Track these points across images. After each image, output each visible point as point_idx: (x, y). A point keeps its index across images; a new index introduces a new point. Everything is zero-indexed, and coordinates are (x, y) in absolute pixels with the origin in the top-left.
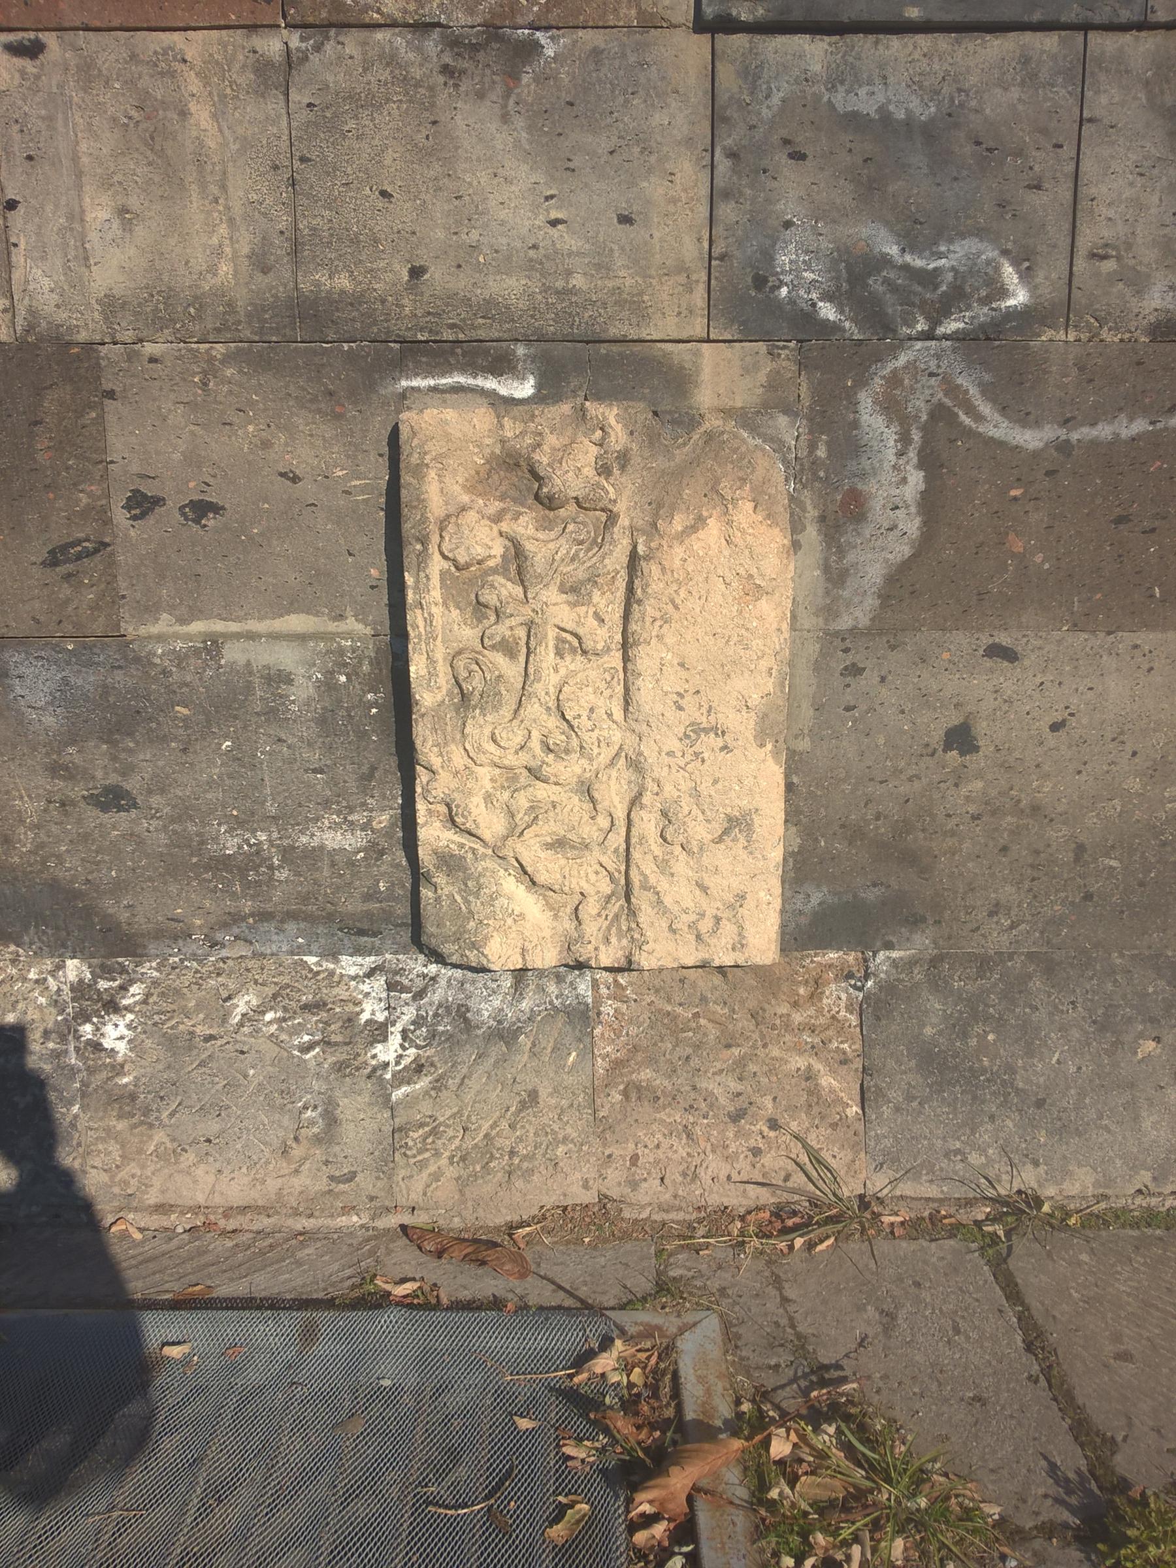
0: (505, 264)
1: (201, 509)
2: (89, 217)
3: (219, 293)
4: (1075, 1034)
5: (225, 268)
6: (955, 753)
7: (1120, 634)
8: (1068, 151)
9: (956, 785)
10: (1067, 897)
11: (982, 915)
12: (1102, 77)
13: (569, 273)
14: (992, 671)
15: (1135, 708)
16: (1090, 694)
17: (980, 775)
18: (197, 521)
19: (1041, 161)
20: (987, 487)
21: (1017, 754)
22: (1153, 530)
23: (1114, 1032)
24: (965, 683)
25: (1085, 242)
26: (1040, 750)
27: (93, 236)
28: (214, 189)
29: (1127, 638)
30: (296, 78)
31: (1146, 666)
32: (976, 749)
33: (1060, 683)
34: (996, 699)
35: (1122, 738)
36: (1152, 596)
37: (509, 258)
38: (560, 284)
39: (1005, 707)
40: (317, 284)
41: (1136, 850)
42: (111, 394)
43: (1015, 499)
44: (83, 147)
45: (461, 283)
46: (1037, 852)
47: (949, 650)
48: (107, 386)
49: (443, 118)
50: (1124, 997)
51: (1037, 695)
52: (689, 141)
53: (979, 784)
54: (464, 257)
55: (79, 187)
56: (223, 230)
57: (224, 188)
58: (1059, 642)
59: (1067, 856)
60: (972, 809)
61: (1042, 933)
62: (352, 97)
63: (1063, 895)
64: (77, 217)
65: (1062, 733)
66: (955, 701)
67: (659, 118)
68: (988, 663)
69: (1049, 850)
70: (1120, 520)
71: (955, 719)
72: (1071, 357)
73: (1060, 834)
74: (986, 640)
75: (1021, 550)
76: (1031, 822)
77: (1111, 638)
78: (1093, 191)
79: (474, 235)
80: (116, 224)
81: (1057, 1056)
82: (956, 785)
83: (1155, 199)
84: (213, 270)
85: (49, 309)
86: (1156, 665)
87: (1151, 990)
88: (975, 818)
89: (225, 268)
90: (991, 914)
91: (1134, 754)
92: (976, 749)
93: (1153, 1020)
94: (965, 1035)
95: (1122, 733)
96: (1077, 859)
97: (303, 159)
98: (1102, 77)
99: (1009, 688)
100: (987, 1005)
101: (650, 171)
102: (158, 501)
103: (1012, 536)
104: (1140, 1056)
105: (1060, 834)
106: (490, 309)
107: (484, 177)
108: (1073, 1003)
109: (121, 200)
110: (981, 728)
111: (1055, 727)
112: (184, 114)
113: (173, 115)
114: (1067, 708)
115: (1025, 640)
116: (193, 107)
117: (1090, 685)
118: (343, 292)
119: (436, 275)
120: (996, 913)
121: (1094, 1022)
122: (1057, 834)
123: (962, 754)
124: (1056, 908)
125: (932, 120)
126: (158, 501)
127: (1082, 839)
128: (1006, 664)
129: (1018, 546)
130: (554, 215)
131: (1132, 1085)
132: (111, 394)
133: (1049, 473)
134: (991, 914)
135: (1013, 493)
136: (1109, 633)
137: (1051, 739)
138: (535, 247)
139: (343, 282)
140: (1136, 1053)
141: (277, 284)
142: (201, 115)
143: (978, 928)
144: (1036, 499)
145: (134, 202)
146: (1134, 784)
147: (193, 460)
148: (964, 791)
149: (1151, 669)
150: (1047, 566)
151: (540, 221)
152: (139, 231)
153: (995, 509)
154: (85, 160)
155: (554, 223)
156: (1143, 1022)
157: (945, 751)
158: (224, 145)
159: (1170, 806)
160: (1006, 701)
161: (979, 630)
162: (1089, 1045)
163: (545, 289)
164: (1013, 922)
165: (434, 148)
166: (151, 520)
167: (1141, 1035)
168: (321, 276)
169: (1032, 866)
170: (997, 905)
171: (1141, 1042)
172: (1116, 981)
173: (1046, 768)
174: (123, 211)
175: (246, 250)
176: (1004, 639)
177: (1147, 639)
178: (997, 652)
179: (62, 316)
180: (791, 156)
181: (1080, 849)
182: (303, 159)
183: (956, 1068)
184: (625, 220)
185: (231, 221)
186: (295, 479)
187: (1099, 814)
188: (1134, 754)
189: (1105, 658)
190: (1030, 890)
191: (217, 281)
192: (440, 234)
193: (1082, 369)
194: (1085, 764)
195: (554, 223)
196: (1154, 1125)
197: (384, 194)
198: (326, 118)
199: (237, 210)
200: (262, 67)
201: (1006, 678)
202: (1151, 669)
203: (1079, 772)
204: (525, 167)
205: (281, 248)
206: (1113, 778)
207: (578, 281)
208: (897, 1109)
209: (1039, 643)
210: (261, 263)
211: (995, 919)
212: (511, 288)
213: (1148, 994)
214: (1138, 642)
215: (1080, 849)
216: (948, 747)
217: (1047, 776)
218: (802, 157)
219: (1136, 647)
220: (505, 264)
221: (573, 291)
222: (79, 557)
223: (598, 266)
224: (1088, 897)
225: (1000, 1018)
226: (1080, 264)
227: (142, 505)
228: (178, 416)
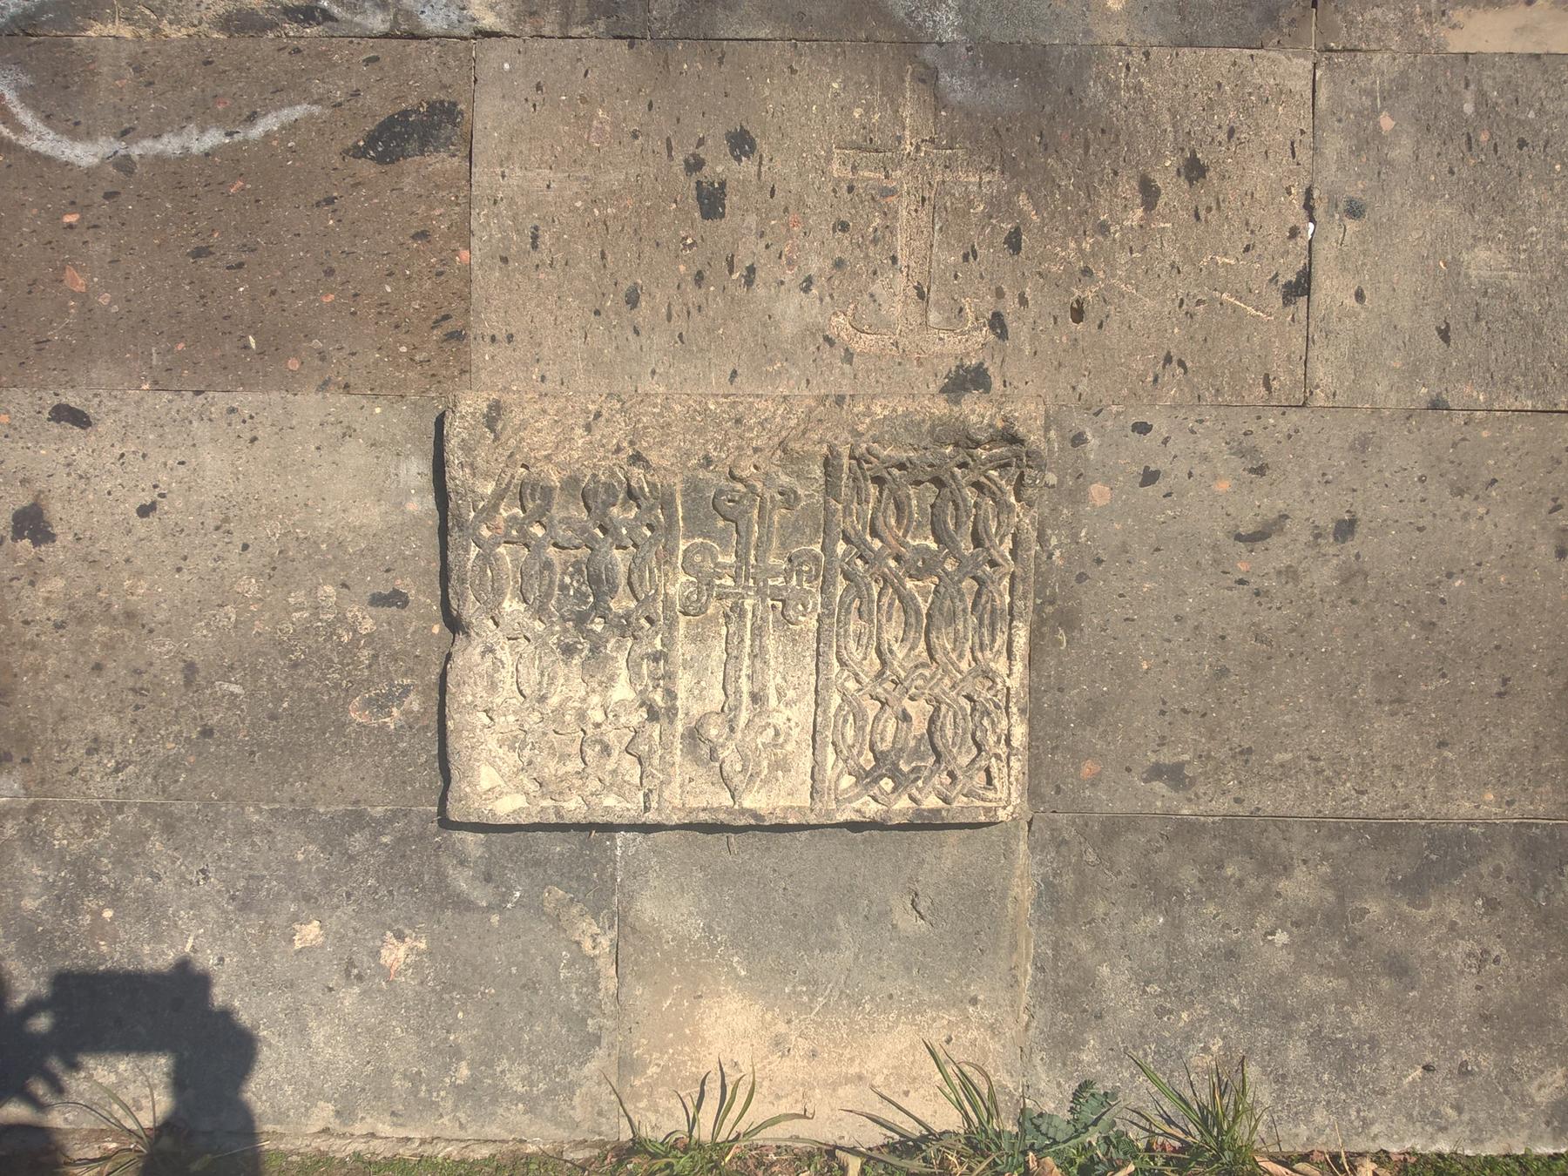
4: (211, 913)
6: (27, 542)
7: (211, 394)
9: (32, 583)
10: (181, 732)
11: (80, 752)
14: (61, 439)
15: (240, 488)
16: (182, 470)
17: (59, 571)
20: (35, 211)
21: (101, 545)
22: (240, 266)
23: (260, 913)
24: (30, 453)
29: (220, 401)
31: (247, 436)
32: (51, 538)
33: (144, 456)
34: (69, 474)
35: (226, 526)
36: (247, 347)
39: (82, 485)
41: (261, 671)
43: (70, 226)
46: (138, 672)
47: (8, 412)
50: (267, 866)
51: (117, 469)
53: (58, 584)
58: (138, 403)
59: (177, 679)
60: (55, 614)
61: (155, 778)
63: (176, 728)
65: (153, 519)
66: (20, 476)
68: (56, 429)
69: (153, 670)
70: (199, 253)
71: (24, 500)
72: (123, 55)
73: (164, 649)
74: (51, 401)
75: (83, 289)
76: (127, 632)
77: (200, 399)
81: (191, 940)
82: (32, 583)
86: (260, 433)
87: (300, 857)
88: (59, 626)
90: (90, 752)
91: (245, 547)
92: (51, 538)
93: (307, 898)
94: (74, 911)
95: (226, 520)
96: (188, 682)
99: (83, 462)
100: (97, 872)
104: (298, 945)
105: (164, 649)
108: (203, 871)
110: (55, 510)
111: (145, 511)
114: (155, 487)
115: (97, 400)
117: (181, 459)
120: (97, 750)
121: (233, 898)
122: (161, 649)
123: (36, 543)
124: (169, 746)
127: (190, 656)
128: (77, 430)
131: (291, 985)
133: (109, 196)
134: (90, 752)
135: (69, 219)
136: (198, 393)
137: (140, 526)
140: (291, 941)
143: (76, 770)
144: (95, 226)
146: (250, 587)
148: (42, 591)
149: (253, 440)
150: (115, 309)
153: (48, 238)
156: (295, 899)
157: (14, 539)
159: (297, 615)
160: (81, 477)
161: (44, 388)
162: (231, 927)
164: (118, 763)
167: (295, 918)
169: (133, 689)
170: (96, 740)
171: (297, 927)
172: (253, 844)
173: (138, 562)
176: (71, 399)
177: (245, 400)
181: (190, 669)
187: (208, 624)
188: (245, 547)
189: (195, 424)
190: (134, 722)
193: (138, 70)
194: (185, 558)
196: (328, 1040)
201: (77, 446)
202: (253, 440)
203: (179, 570)
206: (222, 578)
209: (114, 404)
211: (96, 758)
213: (298, 863)
214: (235, 405)
215: (190, 669)
216: (18, 534)
217: (139, 574)
219: (232, 410)
224: (207, 732)
225: (117, 890)
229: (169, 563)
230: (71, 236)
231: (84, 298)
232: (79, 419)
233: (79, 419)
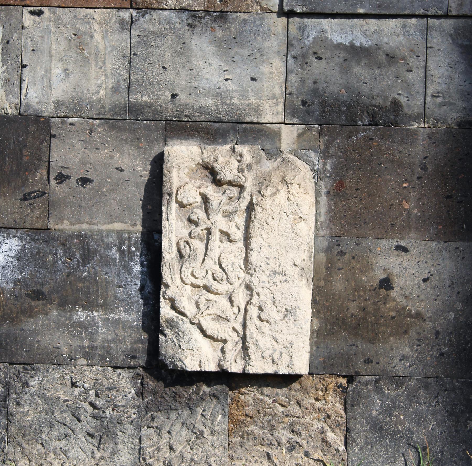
0: (208, 94)
2: (53, 71)
5: (102, 92)
8: (422, 58)
12: (434, 32)
16: (439, 267)
21: (410, 291)
27: (54, 78)
28: (100, 64)
37: (209, 92)
38: (228, 102)
40: (136, 99)
44: (54, 47)
45: (190, 100)
55: (50, 61)
56: (103, 78)
57: (104, 63)
64: (48, 71)
65: (428, 283)
68: (396, 253)
74: (395, 243)
78: (433, 73)
79: (196, 84)
80: (63, 74)
84: (98, 92)
85: (35, 104)
89: (102, 92)
97: (135, 54)
99: (405, 264)
101: (263, 62)
103: (404, 202)
106: (201, 110)
109: (65, 66)
111: (425, 280)
112: (92, 37)
113: (87, 37)
116: (95, 35)
118: (146, 102)
119: (182, 97)
125: (370, 47)
129: (407, 206)
138: (219, 88)
139: (146, 98)
141: (121, 98)
142: (98, 38)
145: (70, 67)
148: (388, 306)
151: (222, 78)
152: (71, 77)
154: (54, 52)
155: (227, 80)
158: (105, 48)
163: (222, 103)
165: (183, 52)
168: (138, 96)
174: (66, 70)
175: (110, 85)
176: (402, 243)
178: (399, 248)
179: (39, 106)
180: (316, 58)
182: (135, 54)
183: (387, 430)
184: (253, 79)
185: (106, 75)
191: (99, 96)
192: (184, 83)
195: (227, 80)
197: (164, 68)
199: (109, 71)
200: (122, 22)
205: (124, 85)
207: (235, 101)
208: (361, 449)
212: (209, 103)
218: (321, 59)
220: (208, 94)
221: (233, 104)
223: (242, 96)
229: (432, 298)
230: (405, 191)
231: (408, 211)
232: (405, 250)
233: (405, 250)
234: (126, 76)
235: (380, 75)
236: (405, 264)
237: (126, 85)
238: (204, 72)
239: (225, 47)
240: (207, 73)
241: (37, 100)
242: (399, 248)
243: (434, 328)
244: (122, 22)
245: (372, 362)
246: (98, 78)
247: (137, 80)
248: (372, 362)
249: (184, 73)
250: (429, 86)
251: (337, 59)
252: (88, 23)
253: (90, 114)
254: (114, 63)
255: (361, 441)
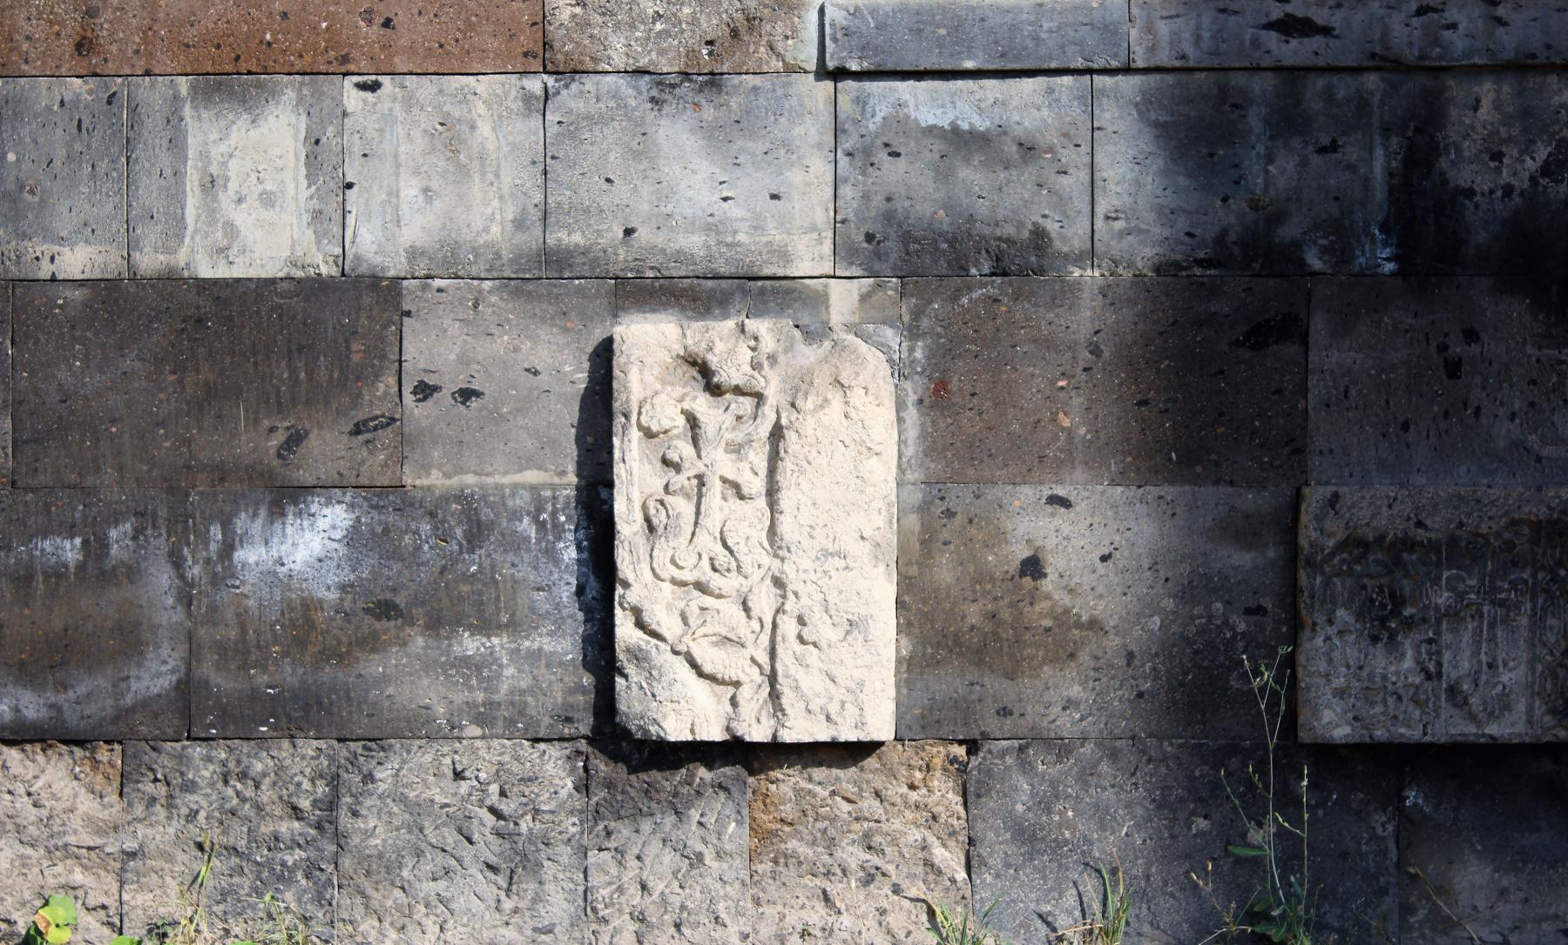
0: (691, 227)
1: (466, 395)
2: (402, 194)
3: (488, 245)
8: (1086, 148)
12: (1105, 100)
13: (735, 232)
16: (1128, 534)
18: (463, 403)
19: (1068, 156)
25: (1102, 208)
26: (1093, 577)
27: (405, 207)
28: (491, 177)
30: (550, 105)
38: (729, 239)
42: (408, 314)
44: (402, 148)
45: (659, 239)
48: (406, 307)
49: (651, 131)
52: (819, 146)
54: (663, 222)
55: (397, 175)
56: (496, 203)
57: (497, 176)
62: (589, 117)
64: (394, 193)
65: (1110, 563)
67: (798, 130)
68: (1049, 509)
74: (1047, 492)
78: (1105, 175)
79: (669, 209)
80: (421, 198)
83: (1150, 179)
84: (486, 230)
85: (370, 255)
89: (495, 229)
93: (1201, 800)
96: (1129, 665)
97: (553, 158)
98: (1105, 100)
101: (792, 164)
102: (436, 389)
103: (1061, 415)
106: (679, 256)
107: (677, 169)
109: (425, 183)
111: (1104, 559)
112: (473, 127)
113: (465, 128)
116: (479, 123)
118: (577, 245)
119: (643, 235)
125: (988, 130)
126: (436, 389)
129: (1066, 423)
130: (725, 194)
132: (408, 314)
133: (1085, 370)
139: (577, 238)
141: (531, 239)
142: (485, 128)
145: (434, 185)
147: (464, 361)
148: (1038, 608)
151: (716, 197)
152: (437, 203)
154: (402, 157)
155: (725, 199)
158: (499, 148)
163: (719, 243)
165: (642, 151)
166: (430, 402)
174: (426, 190)
175: (511, 217)
176: (1060, 491)
178: (1055, 500)
179: (378, 260)
180: (890, 154)
182: (553, 158)
183: (1043, 839)
184: (774, 197)
185: (501, 197)
186: (536, 373)
191: (489, 237)
192: (646, 207)
195: (725, 199)
197: (608, 180)
198: (570, 130)
199: (506, 190)
200: (528, 98)
204: (705, 163)
205: (535, 215)
208: (998, 876)
210: (520, 224)
212: (693, 242)
216: (1023, 574)
218: (898, 155)
220: (691, 227)
221: (738, 244)
222: (375, 429)
223: (756, 228)
226: (1100, 224)
227: (425, 391)
228: (455, 329)
229: (1119, 590)
230: (1062, 395)
231: (1069, 430)
232: (1065, 503)
233: (1065, 503)
234: (538, 197)
235: (1009, 182)
236: (1066, 529)
237: (540, 214)
238: (683, 186)
239: (719, 137)
240: (689, 188)
241: (374, 248)
242: (1055, 500)
243: (1125, 646)
244: (528, 98)
245: (1011, 713)
246: (487, 203)
247: (559, 204)
248: (1011, 713)
249: (646, 190)
250: (1099, 198)
251: (929, 155)
252: (465, 101)
253: (474, 271)
254: (516, 176)
255: (996, 861)
